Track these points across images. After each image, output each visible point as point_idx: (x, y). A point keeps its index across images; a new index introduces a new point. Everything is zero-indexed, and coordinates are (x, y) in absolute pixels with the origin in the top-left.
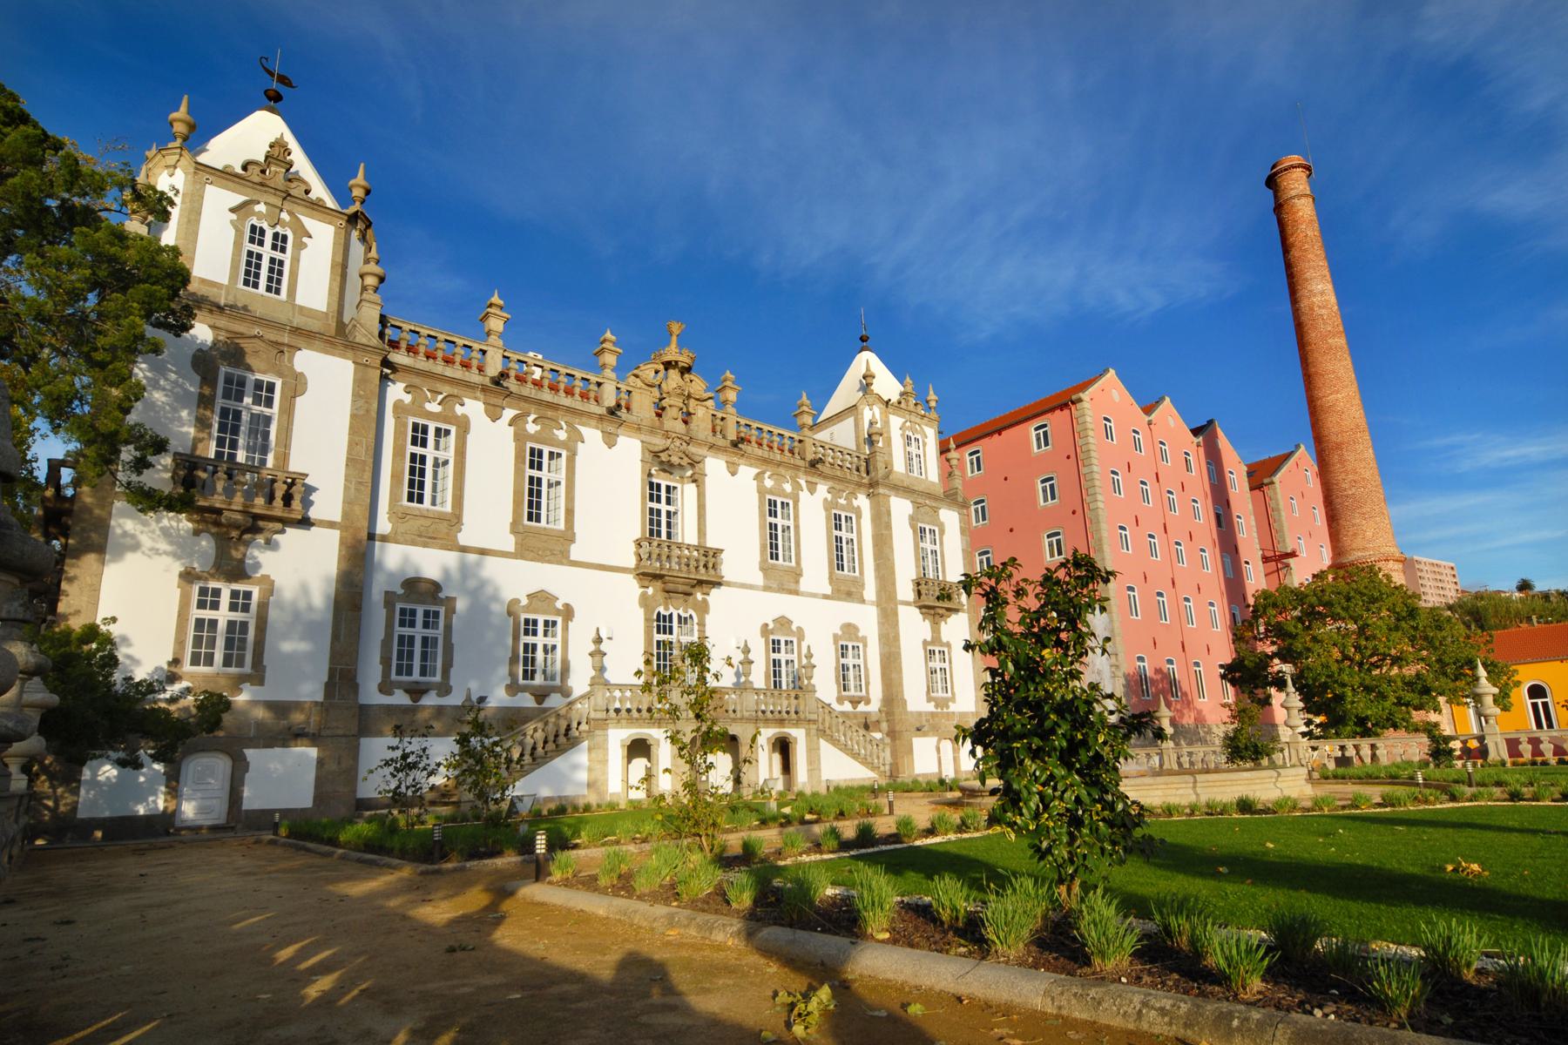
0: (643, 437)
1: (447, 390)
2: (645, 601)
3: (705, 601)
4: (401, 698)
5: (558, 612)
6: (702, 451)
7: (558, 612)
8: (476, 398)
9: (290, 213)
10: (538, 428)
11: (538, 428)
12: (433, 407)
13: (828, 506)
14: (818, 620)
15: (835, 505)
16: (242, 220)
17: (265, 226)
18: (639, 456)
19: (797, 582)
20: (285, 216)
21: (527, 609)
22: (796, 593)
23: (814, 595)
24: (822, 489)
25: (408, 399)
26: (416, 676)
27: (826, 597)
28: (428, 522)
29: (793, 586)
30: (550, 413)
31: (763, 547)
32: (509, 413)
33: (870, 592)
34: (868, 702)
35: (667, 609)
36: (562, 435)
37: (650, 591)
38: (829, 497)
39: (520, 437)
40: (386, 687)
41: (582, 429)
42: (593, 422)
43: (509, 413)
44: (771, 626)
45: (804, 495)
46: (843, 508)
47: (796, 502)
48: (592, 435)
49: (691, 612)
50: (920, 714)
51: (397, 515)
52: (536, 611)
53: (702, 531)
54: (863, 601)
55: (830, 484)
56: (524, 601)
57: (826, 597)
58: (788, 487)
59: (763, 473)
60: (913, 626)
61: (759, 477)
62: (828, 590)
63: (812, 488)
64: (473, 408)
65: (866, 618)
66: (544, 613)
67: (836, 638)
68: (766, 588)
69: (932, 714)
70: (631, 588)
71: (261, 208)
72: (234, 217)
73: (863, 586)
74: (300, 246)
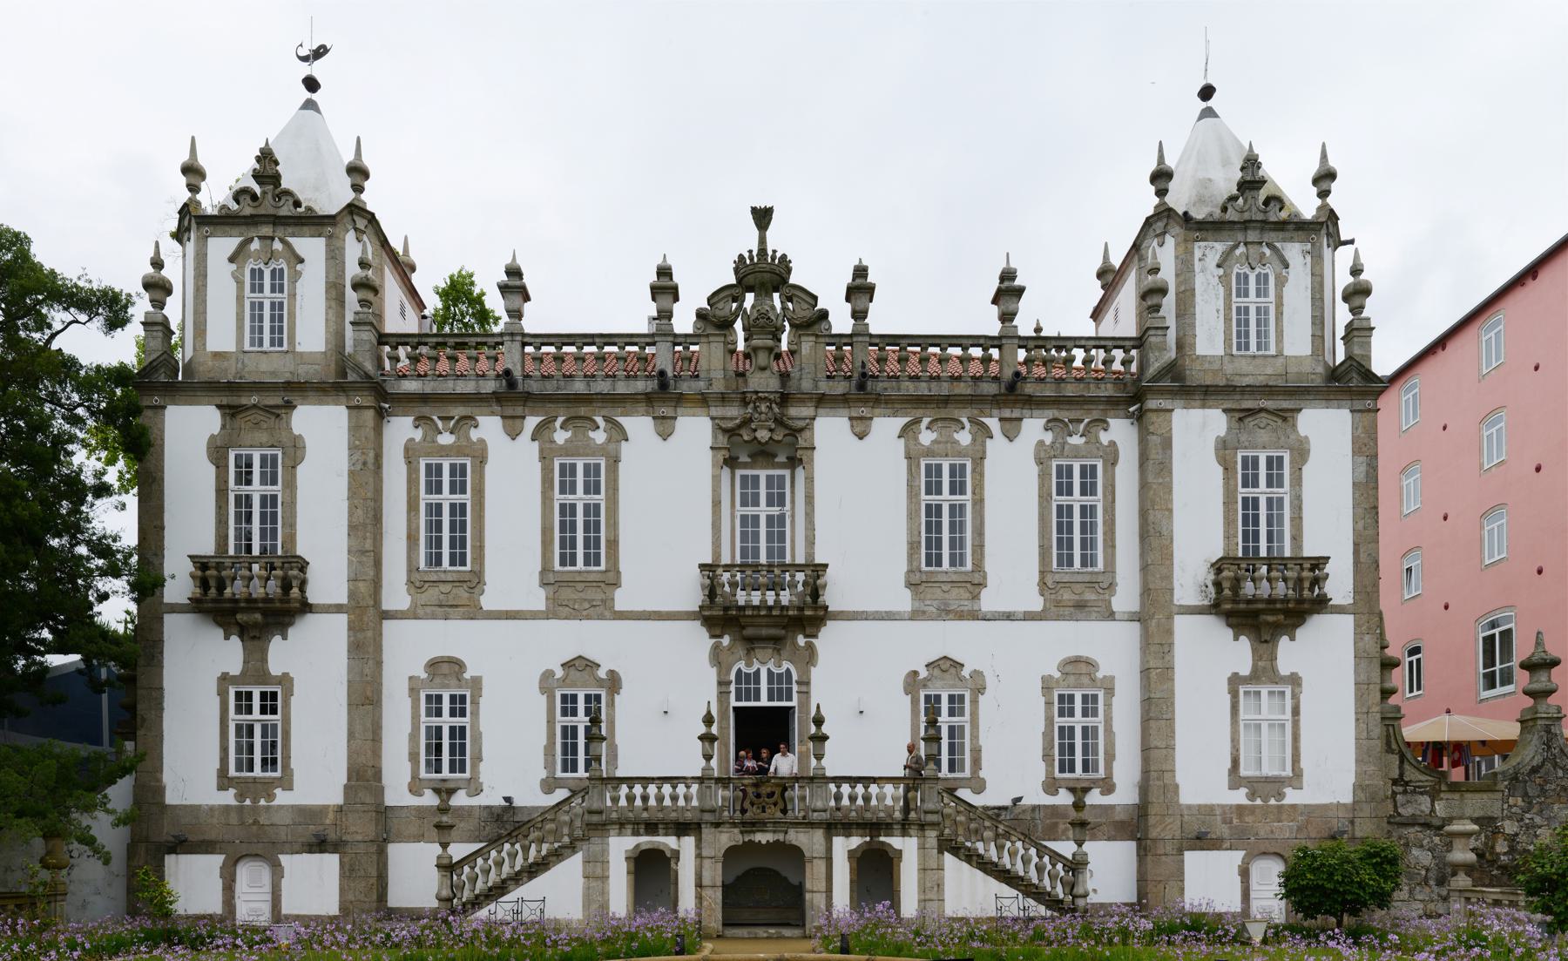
0: (715, 411)
1: (457, 411)
2: (717, 657)
3: (811, 648)
4: (429, 799)
5: (600, 683)
6: (806, 411)
7: (600, 683)
8: (493, 414)
9: (282, 241)
10: (568, 434)
11: (568, 434)
12: (446, 439)
13: (1042, 457)
14: (1014, 663)
15: (1059, 449)
16: (241, 268)
17: (262, 266)
18: (709, 442)
19: (976, 597)
20: (277, 245)
21: (564, 682)
22: (975, 616)
23: (1009, 617)
24: (1034, 428)
25: (418, 435)
26: (446, 773)
27: (1029, 616)
28: (445, 588)
29: (967, 605)
30: (583, 411)
31: (913, 547)
32: (532, 422)
33: (1126, 597)
34: (1108, 787)
35: (749, 665)
36: (599, 437)
37: (726, 641)
38: (1048, 438)
39: (545, 458)
40: (415, 787)
41: (621, 420)
42: (642, 407)
43: (532, 422)
44: (923, 673)
45: (997, 447)
46: (1076, 453)
47: (979, 460)
48: (639, 426)
49: (786, 665)
50: (1209, 810)
51: (416, 583)
52: (573, 685)
53: (810, 542)
54: (1111, 616)
55: (1050, 413)
56: (559, 673)
57: (1029, 616)
58: (964, 438)
59: (917, 421)
60: (1208, 653)
61: (907, 432)
62: (1037, 604)
63: (1011, 429)
64: (489, 427)
65: (1112, 647)
66: (584, 685)
67: (1047, 685)
68: (916, 615)
69: (1240, 808)
70: (698, 640)
71: (255, 245)
72: (234, 267)
73: (1112, 586)
74: (296, 276)
